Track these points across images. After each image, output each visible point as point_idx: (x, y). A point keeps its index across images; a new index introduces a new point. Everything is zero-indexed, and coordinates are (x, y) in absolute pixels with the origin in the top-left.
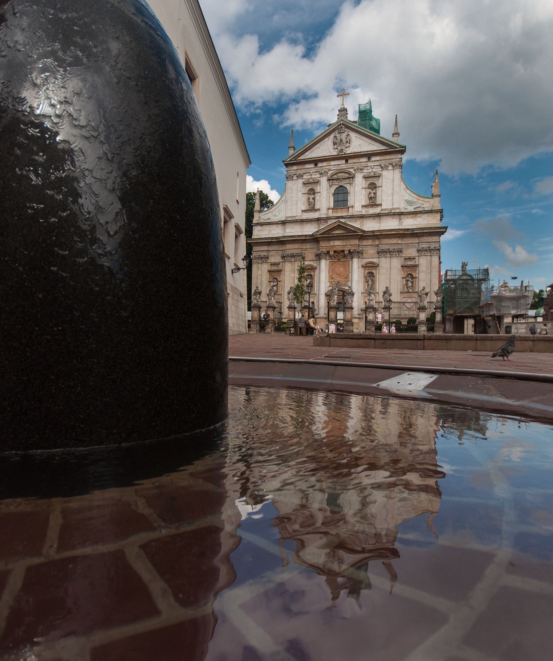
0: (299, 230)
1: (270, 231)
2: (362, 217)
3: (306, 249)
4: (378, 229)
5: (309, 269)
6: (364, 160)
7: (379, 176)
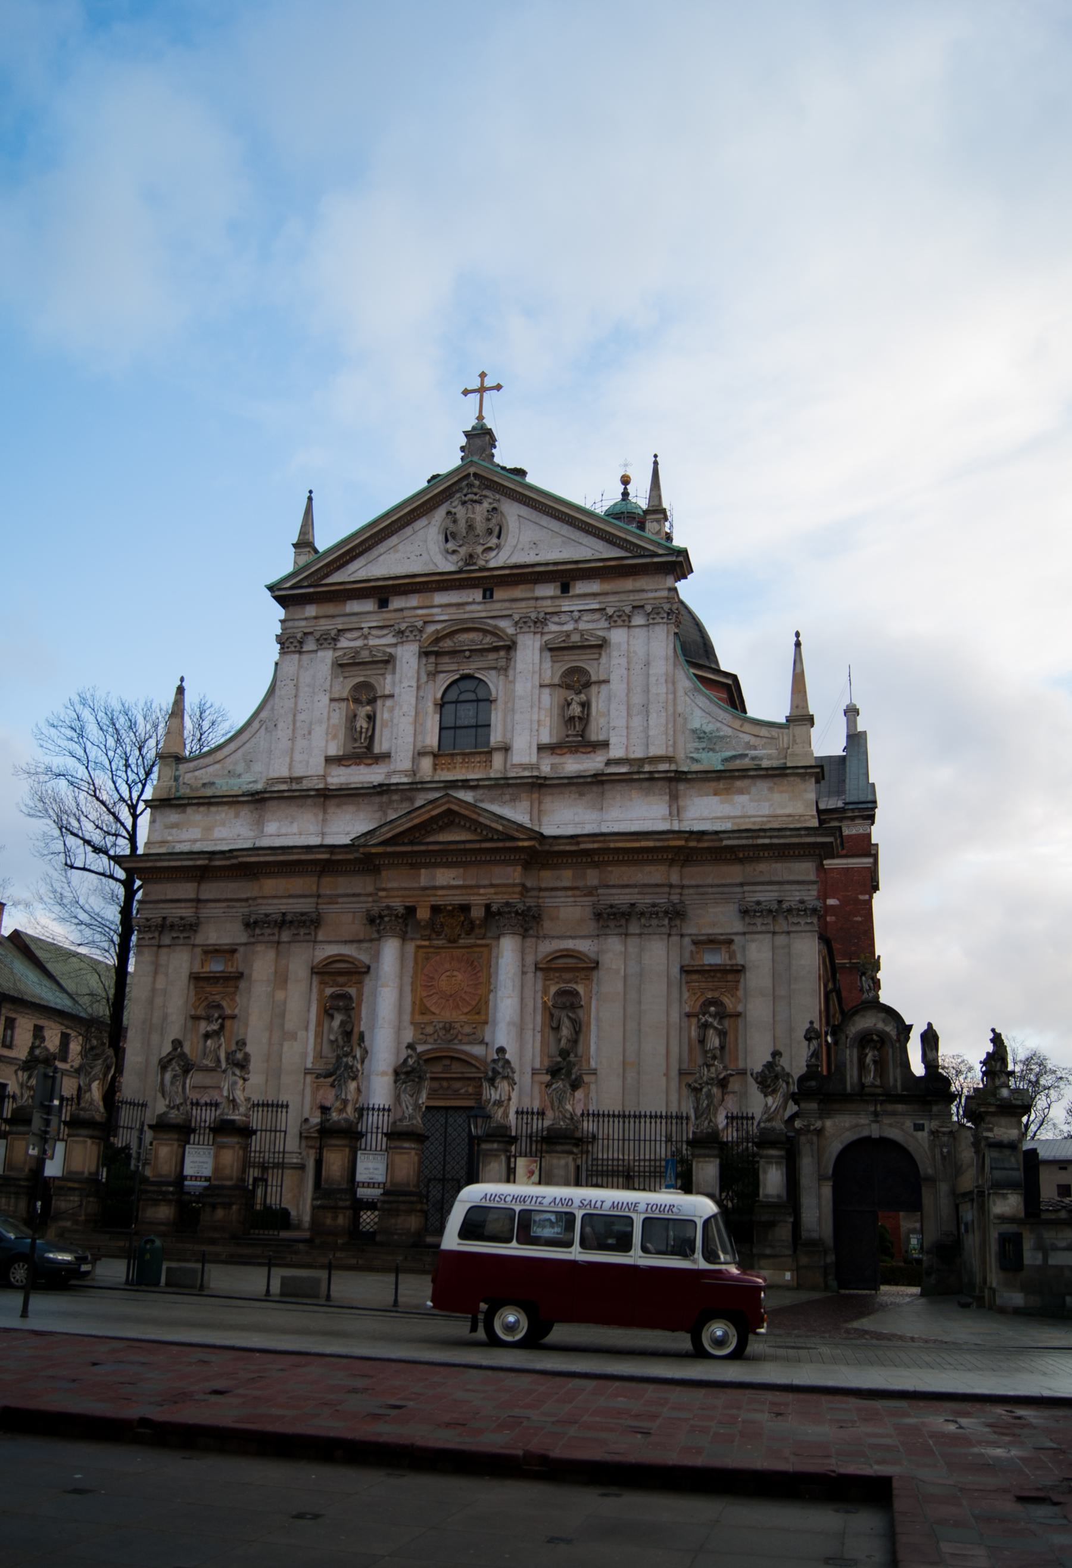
0: (313, 828)
1: (208, 829)
3: (333, 899)
4: (597, 831)
5: (340, 973)
6: (548, 590)
7: (600, 646)
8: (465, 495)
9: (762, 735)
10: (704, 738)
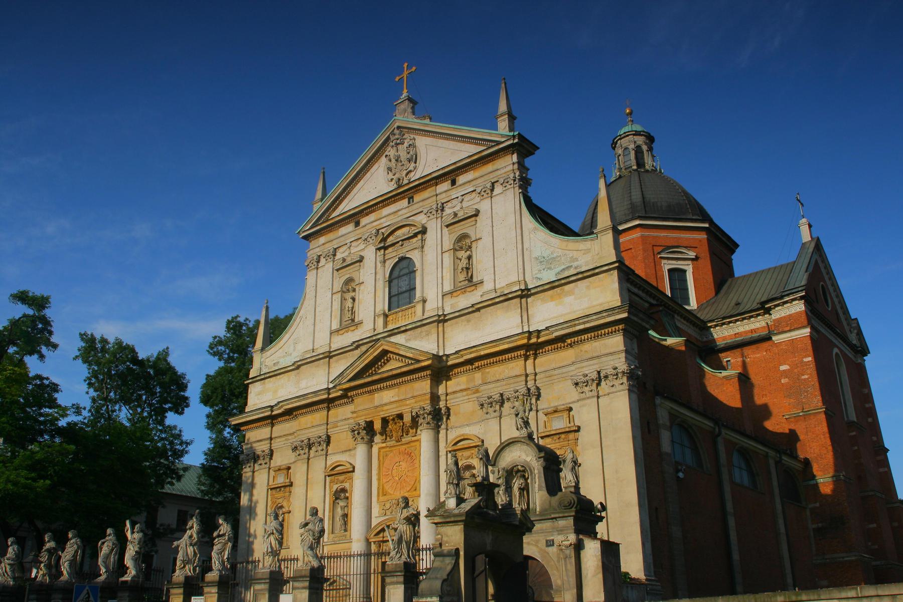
2: (442, 320)
6: (445, 186)
9: (580, 249)
10: (543, 261)
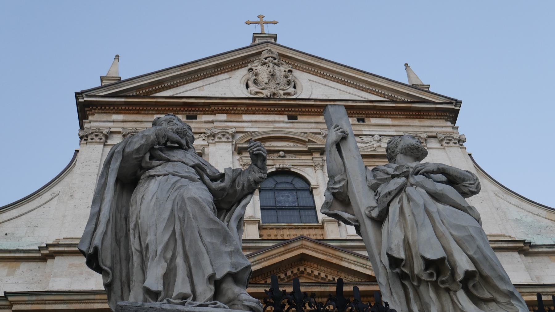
8: (266, 59)
